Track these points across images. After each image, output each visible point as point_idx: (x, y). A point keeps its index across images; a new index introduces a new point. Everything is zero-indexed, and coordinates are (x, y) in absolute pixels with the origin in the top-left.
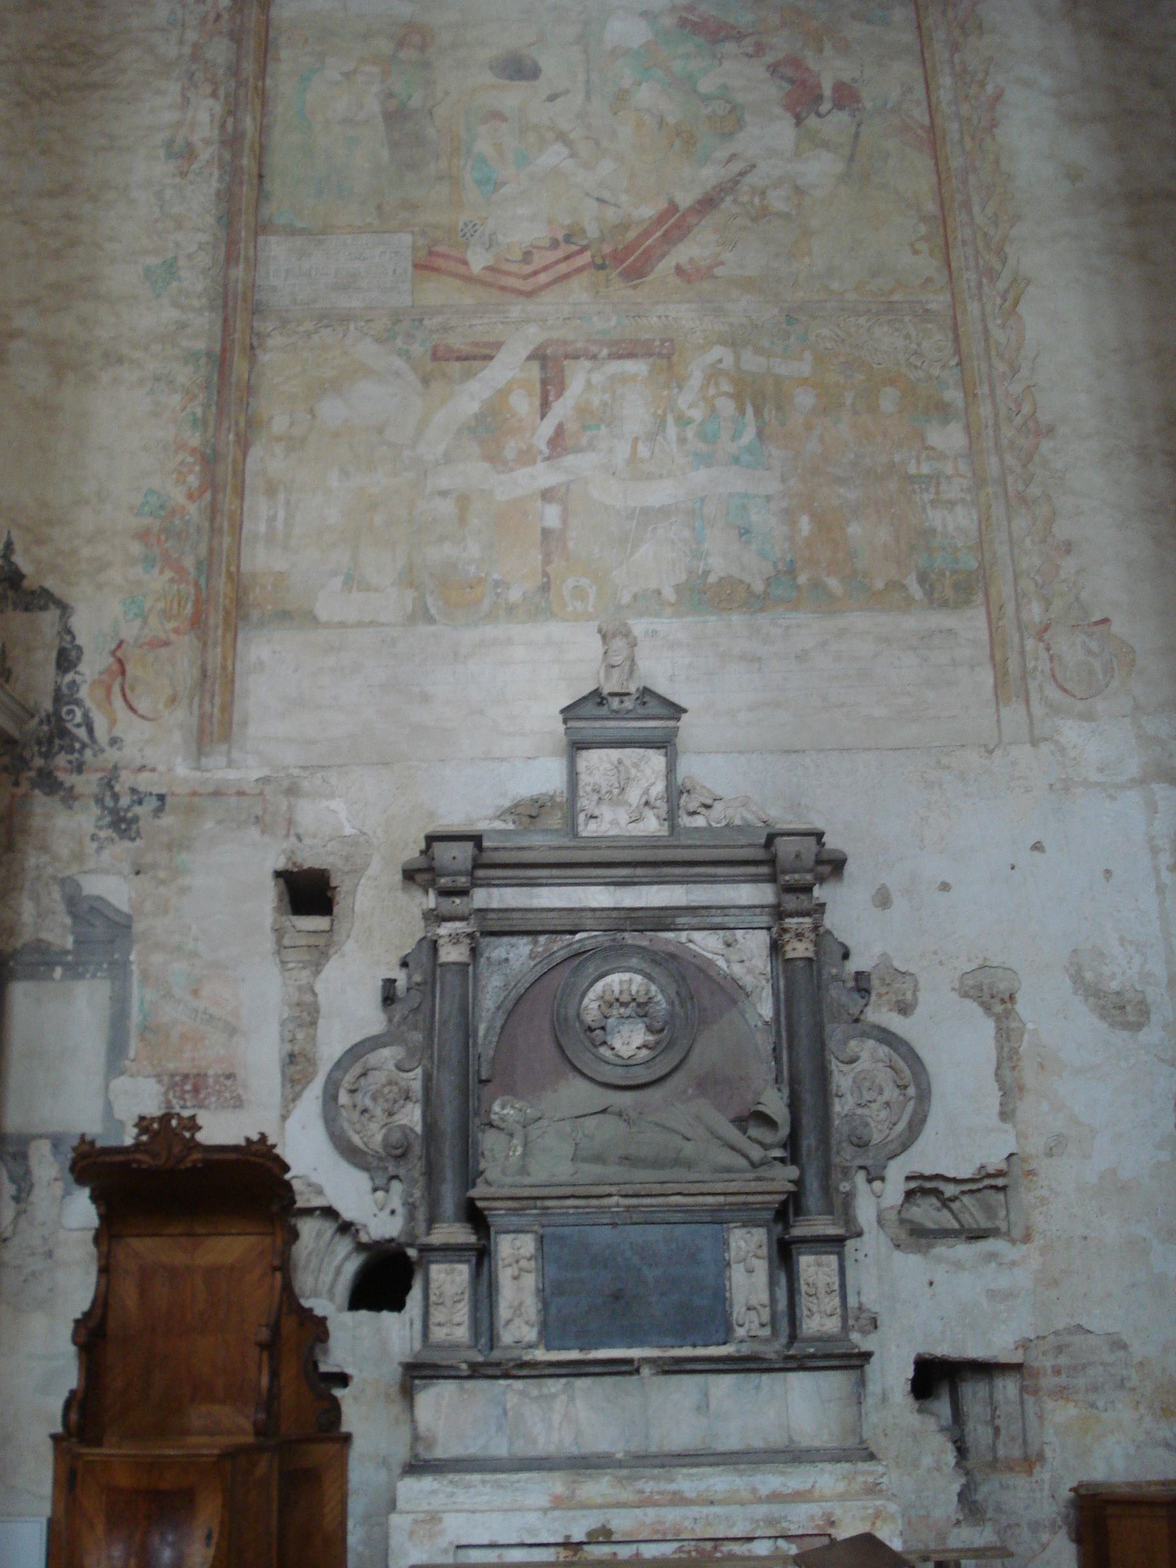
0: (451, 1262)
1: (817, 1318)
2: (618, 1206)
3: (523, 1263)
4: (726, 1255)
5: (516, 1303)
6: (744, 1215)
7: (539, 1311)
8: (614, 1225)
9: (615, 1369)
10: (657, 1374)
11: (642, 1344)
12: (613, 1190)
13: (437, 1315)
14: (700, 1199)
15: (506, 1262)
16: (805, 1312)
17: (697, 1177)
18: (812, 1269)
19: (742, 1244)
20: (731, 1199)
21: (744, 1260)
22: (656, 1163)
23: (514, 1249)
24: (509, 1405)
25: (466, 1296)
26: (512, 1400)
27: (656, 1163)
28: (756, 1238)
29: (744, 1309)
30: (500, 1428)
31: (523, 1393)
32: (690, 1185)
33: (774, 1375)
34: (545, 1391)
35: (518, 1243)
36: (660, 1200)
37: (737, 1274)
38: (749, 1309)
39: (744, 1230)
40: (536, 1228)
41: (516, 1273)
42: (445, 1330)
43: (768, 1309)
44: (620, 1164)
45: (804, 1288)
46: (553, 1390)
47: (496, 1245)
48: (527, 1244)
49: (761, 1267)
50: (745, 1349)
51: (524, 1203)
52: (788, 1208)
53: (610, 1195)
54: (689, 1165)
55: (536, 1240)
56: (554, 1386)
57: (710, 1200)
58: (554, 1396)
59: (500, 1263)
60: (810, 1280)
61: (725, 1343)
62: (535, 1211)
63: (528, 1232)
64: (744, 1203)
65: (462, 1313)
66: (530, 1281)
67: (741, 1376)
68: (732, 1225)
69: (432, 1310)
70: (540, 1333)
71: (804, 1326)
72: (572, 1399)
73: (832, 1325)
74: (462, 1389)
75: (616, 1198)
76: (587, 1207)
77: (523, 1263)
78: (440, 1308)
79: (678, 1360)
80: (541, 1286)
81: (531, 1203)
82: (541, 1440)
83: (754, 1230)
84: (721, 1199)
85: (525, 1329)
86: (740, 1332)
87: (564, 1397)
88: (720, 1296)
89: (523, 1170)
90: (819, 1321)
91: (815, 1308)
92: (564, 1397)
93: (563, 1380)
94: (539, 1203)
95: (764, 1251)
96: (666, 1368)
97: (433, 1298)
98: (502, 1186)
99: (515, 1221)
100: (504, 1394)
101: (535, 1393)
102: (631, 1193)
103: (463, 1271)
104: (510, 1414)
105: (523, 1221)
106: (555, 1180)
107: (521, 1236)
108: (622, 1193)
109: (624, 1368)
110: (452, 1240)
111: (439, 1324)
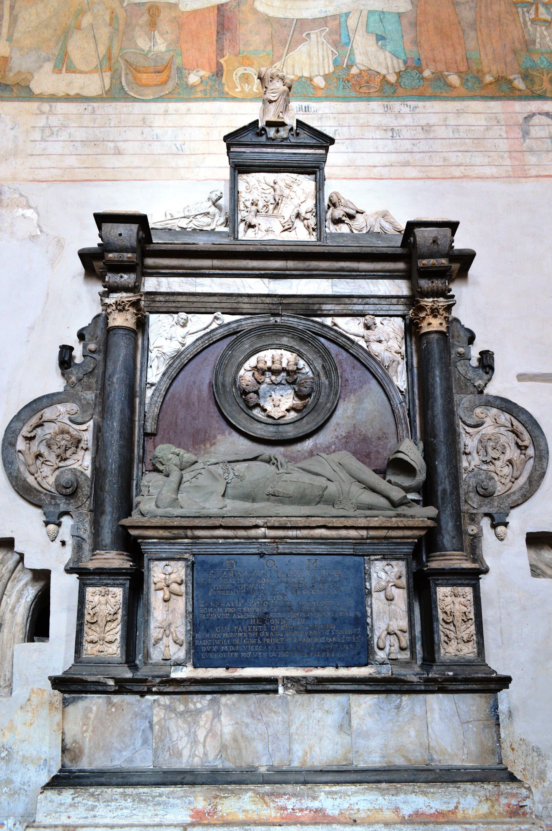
0: (107, 585)
1: (454, 643)
2: (265, 537)
3: (175, 587)
4: (367, 584)
5: (165, 624)
6: (383, 548)
7: (187, 631)
8: (261, 555)
9: (261, 687)
10: (299, 692)
11: (285, 664)
12: (260, 522)
13: (90, 634)
14: (344, 533)
15: (159, 585)
16: (443, 638)
17: (342, 512)
18: (449, 600)
19: (383, 575)
20: (372, 533)
21: (385, 589)
22: (302, 499)
23: (166, 575)
24: (155, 719)
25: (119, 616)
26: (158, 714)
27: (302, 499)
28: (396, 569)
29: (386, 633)
30: (145, 742)
31: (169, 709)
32: (334, 520)
33: (414, 696)
34: (191, 706)
35: (169, 569)
36: (305, 533)
37: (377, 602)
38: (389, 634)
39: (385, 563)
40: (186, 556)
41: (167, 597)
42: (98, 647)
43: (407, 635)
44: (268, 500)
45: (441, 616)
46: (199, 706)
47: (149, 570)
48: (178, 570)
49: (400, 596)
50: (386, 671)
51: (175, 532)
52: (428, 542)
53: (257, 527)
54: (332, 502)
55: (187, 566)
56: (200, 702)
57: (353, 533)
58: (199, 712)
59: (153, 587)
60: (447, 609)
61: (366, 665)
62: (186, 541)
63: (179, 559)
64: (385, 538)
65: (115, 631)
66: (180, 605)
67: (382, 696)
68: (373, 558)
69: (86, 628)
70: (188, 652)
71: (442, 651)
72: (217, 715)
73: (468, 651)
74: (109, 703)
75: (263, 529)
76: (236, 538)
77: (175, 587)
78: (93, 627)
79: (321, 680)
80: (190, 609)
81: (181, 532)
82: (186, 753)
83: (394, 563)
84: (364, 533)
85: (174, 648)
86: (381, 655)
87: (210, 713)
88: (361, 622)
89: (175, 502)
90: (454, 648)
91: (452, 635)
92: (210, 713)
93: (209, 697)
94: (189, 533)
95: (403, 581)
96: (309, 688)
97: (87, 618)
98: (156, 516)
99: (166, 549)
100: (151, 708)
101: (182, 708)
102: (277, 524)
103: (117, 594)
104: (157, 727)
105: (176, 549)
106: (205, 512)
107: (172, 563)
108: (269, 524)
109: (268, 687)
110: (107, 566)
111: (92, 642)
